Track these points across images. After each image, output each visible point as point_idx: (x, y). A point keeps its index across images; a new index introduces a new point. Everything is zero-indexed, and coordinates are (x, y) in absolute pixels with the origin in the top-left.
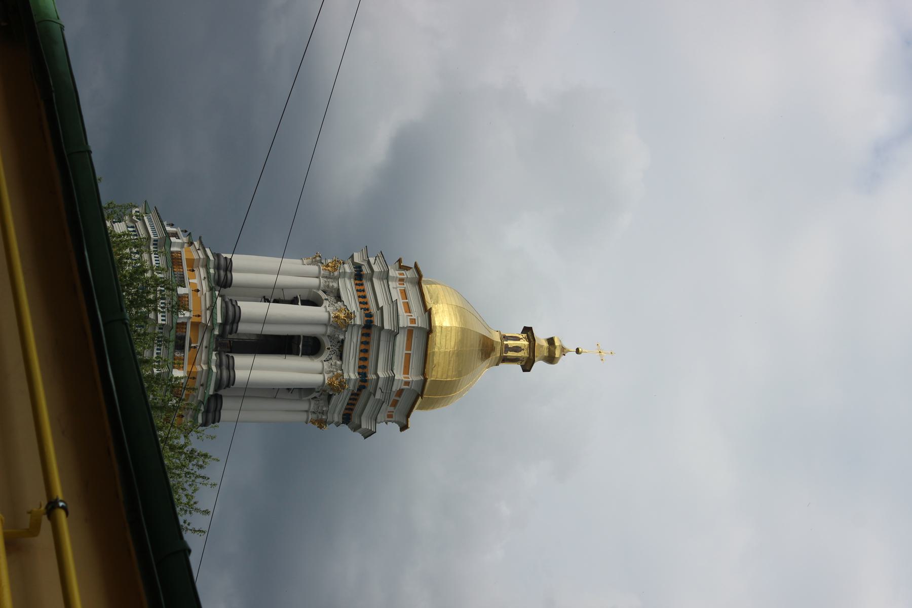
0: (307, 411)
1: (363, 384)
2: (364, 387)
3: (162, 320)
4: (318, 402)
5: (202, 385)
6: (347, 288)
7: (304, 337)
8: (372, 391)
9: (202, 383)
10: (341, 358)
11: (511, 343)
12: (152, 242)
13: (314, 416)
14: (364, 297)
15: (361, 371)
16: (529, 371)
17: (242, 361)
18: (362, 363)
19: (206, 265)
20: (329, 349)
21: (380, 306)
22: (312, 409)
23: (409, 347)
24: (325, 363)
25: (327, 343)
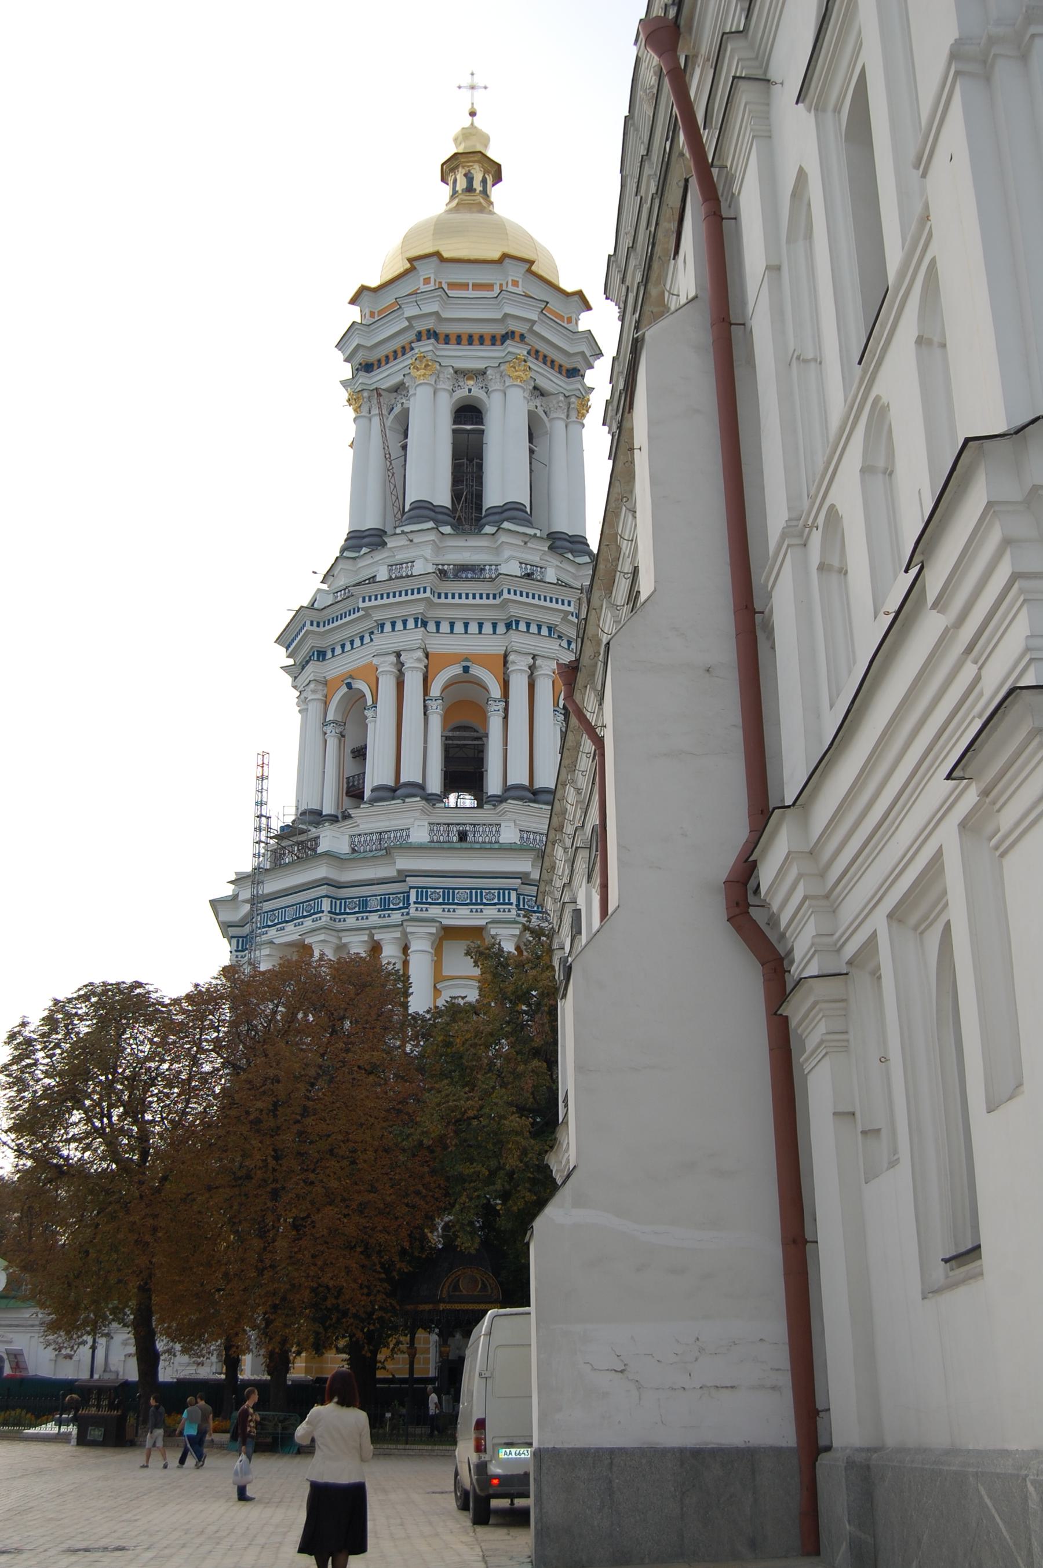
0: (566, 426)
2: (522, 337)
3: (425, 592)
4: (552, 409)
5: (526, 543)
6: (385, 377)
7: (455, 422)
9: (523, 544)
12: (314, 628)
13: (573, 415)
14: (395, 352)
15: (498, 342)
16: (499, 166)
17: (493, 496)
18: (488, 341)
19: (354, 558)
20: (470, 390)
21: (406, 324)
23: (464, 286)
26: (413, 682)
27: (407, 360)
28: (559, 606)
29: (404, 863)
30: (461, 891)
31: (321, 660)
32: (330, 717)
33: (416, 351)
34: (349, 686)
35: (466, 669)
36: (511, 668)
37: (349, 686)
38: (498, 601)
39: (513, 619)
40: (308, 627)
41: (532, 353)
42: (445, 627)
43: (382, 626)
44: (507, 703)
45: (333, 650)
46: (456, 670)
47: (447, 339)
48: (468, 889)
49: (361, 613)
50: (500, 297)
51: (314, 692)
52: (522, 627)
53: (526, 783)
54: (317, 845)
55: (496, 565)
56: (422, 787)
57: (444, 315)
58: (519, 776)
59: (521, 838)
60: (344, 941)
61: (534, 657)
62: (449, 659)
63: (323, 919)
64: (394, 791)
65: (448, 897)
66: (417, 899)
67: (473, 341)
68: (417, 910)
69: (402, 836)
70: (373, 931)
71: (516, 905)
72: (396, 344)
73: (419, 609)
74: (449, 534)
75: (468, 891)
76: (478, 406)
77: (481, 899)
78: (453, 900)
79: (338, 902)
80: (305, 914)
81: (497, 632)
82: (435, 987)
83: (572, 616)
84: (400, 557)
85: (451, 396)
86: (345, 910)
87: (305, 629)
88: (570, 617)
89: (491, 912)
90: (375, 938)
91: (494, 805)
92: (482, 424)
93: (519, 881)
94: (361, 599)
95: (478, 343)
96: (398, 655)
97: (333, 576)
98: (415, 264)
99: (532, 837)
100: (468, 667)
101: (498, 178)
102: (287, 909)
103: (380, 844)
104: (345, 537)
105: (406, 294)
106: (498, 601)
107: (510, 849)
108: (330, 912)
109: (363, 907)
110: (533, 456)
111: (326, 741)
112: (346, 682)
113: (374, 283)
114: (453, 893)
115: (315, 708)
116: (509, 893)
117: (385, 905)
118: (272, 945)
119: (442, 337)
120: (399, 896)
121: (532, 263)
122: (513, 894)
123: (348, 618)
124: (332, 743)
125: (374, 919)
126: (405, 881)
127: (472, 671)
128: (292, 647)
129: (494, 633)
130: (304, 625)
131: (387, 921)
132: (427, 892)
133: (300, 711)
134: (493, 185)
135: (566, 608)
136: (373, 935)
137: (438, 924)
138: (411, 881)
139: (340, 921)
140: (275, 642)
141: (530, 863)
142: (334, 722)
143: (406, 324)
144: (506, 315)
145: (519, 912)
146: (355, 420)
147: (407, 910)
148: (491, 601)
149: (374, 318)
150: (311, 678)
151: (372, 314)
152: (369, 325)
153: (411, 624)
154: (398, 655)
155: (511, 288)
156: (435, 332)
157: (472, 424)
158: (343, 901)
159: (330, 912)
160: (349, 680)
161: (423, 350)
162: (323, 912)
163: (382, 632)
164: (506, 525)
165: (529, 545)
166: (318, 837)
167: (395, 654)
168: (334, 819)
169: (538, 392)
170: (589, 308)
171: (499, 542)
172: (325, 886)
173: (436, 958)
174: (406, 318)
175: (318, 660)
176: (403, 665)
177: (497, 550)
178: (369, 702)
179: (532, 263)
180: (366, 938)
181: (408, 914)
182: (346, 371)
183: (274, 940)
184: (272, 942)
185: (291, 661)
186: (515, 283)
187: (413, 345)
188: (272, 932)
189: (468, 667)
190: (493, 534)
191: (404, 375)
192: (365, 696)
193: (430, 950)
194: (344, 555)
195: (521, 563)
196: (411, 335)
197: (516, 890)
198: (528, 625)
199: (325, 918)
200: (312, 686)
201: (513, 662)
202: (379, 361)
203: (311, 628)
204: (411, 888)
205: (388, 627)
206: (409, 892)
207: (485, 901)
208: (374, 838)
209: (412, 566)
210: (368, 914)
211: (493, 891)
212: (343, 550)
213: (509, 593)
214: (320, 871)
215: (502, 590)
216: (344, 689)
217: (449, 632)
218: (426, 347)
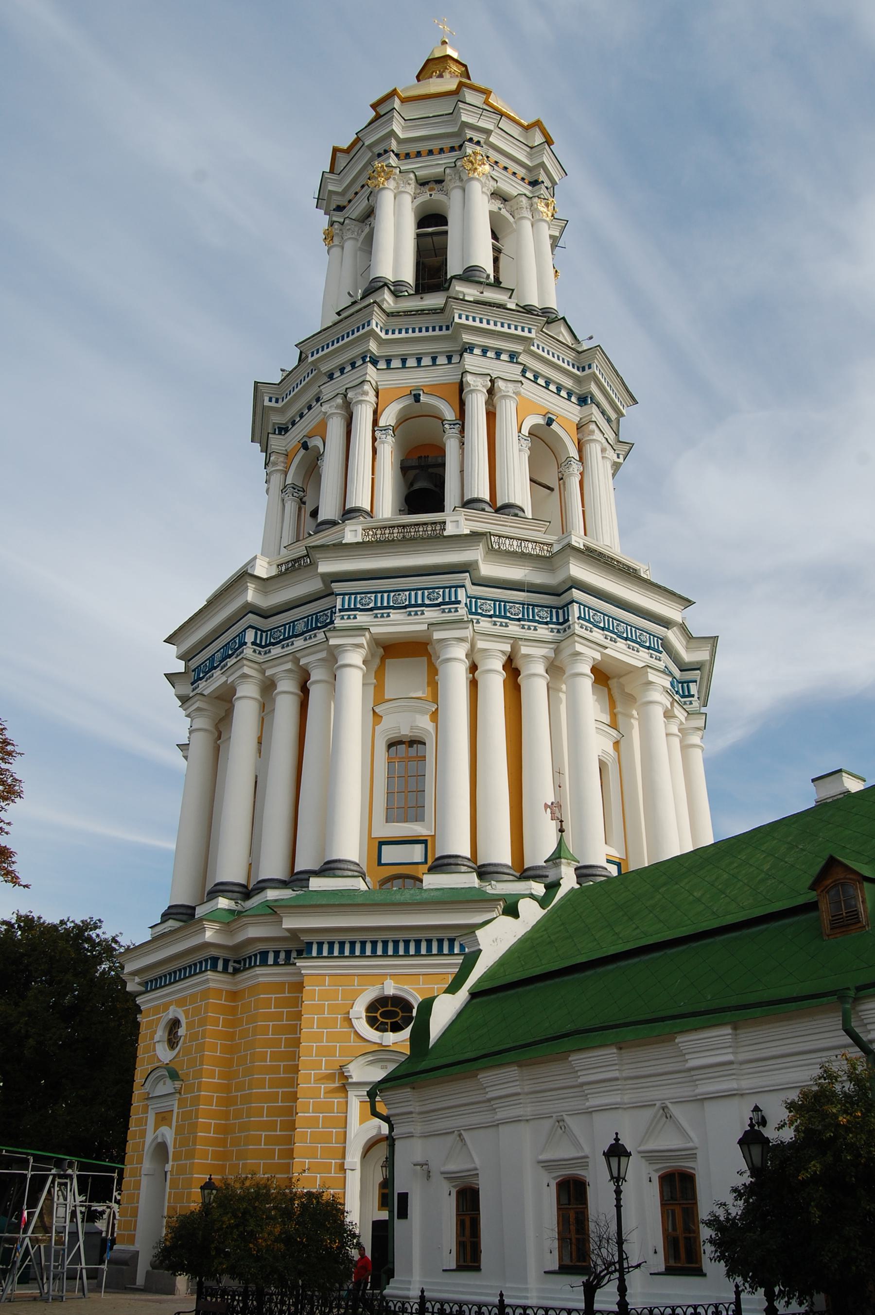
20: (500, 209)
24: (517, 216)
32: (382, 423)
42: (529, 375)
49: (444, 332)
57: (492, 139)
60: (481, 644)
72: (435, 145)
80: (427, 602)
87: (367, 329)
89: (644, 654)
96: (492, 381)
102: (392, 594)
109: (501, 613)
112: (413, 393)
125: (514, 629)
127: (554, 426)
131: (531, 634)
138: (576, 594)
144: (542, 165)
148: (575, 371)
162: (459, 602)
166: (445, 523)
167: (489, 378)
188: (362, 619)
205: (477, 351)
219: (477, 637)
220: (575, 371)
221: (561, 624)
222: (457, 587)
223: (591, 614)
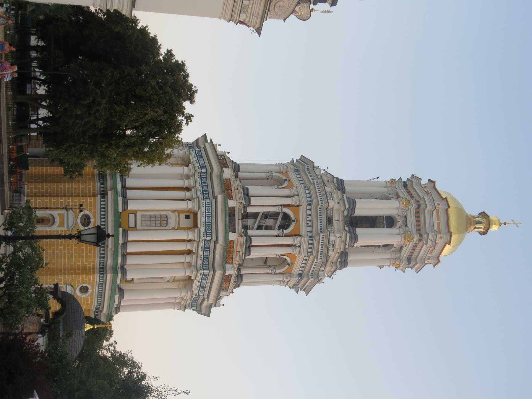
0: (389, 259)
1: (420, 238)
6: (402, 192)
7: (386, 216)
8: (425, 242)
9: (342, 241)
10: (406, 226)
11: (477, 219)
12: (306, 168)
14: (411, 194)
17: (359, 231)
18: (418, 228)
19: (333, 182)
20: (399, 221)
22: (392, 257)
23: (438, 219)
25: (399, 219)
26: (288, 201)
27: (408, 197)
28: (319, 255)
29: (220, 198)
30: (211, 219)
31: (296, 171)
33: (412, 200)
34: (286, 180)
35: (294, 221)
36: (295, 237)
37: (286, 180)
38: (319, 232)
39: (313, 239)
40: (307, 165)
41: (416, 245)
42: (309, 212)
43: (308, 190)
44: (282, 236)
45: (299, 174)
46: (293, 217)
47: (417, 212)
48: (211, 221)
49: (312, 182)
50: (434, 231)
51: (283, 168)
52: (310, 242)
53: (253, 244)
54: (226, 168)
55: (333, 232)
56: (249, 205)
58: (255, 242)
59: (231, 241)
60: (191, 178)
61: (299, 246)
62: (297, 214)
63: (199, 170)
64: (247, 196)
65: (208, 214)
66: (207, 203)
67: (418, 222)
68: (203, 203)
69: (230, 197)
70: (195, 188)
71: (205, 240)
73: (315, 203)
74: (344, 214)
75: (210, 222)
76: (394, 225)
77: (207, 226)
78: (207, 216)
79: (205, 175)
80: (200, 164)
81: (308, 233)
82: (176, 211)
83: (316, 261)
84: (335, 196)
85: (396, 214)
86: (203, 177)
88: (316, 260)
89: (203, 229)
90: (192, 189)
91: (243, 232)
92: (387, 227)
93: (215, 240)
94: (317, 181)
95: (417, 224)
97: (327, 175)
98: (445, 200)
99: (232, 245)
100: (294, 221)
101: (482, 234)
103: (227, 189)
104: (342, 179)
105: (434, 198)
106: (319, 232)
107: (226, 236)
108: (201, 172)
109: (203, 184)
110: (377, 248)
111: (265, 173)
113: (436, 186)
114: (210, 216)
115: (277, 169)
116: (210, 236)
117: (204, 192)
118: (189, 154)
119: (417, 210)
120: (208, 197)
121: (450, 244)
122: (210, 238)
123: (310, 178)
124: (264, 175)
125: (199, 188)
126: (213, 198)
128: (300, 161)
129: (308, 232)
130: (307, 164)
132: (210, 206)
133: (276, 164)
134: (479, 232)
135: (319, 257)
136: (193, 188)
137: (198, 210)
139: (198, 176)
140: (301, 155)
141: (221, 244)
142: (272, 175)
143: (422, 197)
144: (428, 234)
145: (204, 240)
146: (385, 181)
147: (203, 199)
149: (424, 187)
150: (288, 167)
151: (425, 187)
152: (421, 185)
153: (309, 199)
154: (298, 195)
155: (438, 236)
156: (420, 207)
157: (386, 223)
158: (205, 177)
159: (201, 172)
160: (288, 180)
161: (413, 202)
162: (201, 169)
163: (305, 190)
164: (348, 235)
165: (342, 243)
166: (229, 168)
168: (236, 177)
169: (402, 248)
170: (434, 266)
171: (342, 232)
172: (210, 170)
173: (186, 211)
174: (424, 197)
175: (295, 170)
176: (294, 197)
177: (339, 231)
178: (280, 187)
179: (450, 244)
180: (192, 185)
181: (201, 200)
182: (404, 180)
183: (191, 155)
184: (190, 154)
185: (295, 162)
186: (441, 238)
187: (414, 199)
188: (194, 154)
189: (294, 221)
190: (345, 230)
191: (403, 197)
192: (282, 185)
193: (188, 208)
194: (335, 178)
195: (334, 241)
196: (418, 199)
197: (212, 239)
198: (311, 244)
199: (199, 170)
200: (285, 167)
201: (297, 238)
202: (408, 189)
203: (306, 167)
204: (211, 200)
206: (209, 200)
207: (207, 227)
208: (229, 187)
209: (331, 200)
210: (201, 185)
211: (211, 230)
212: (337, 178)
213: (323, 236)
214: (216, 169)
215: (323, 233)
216: (284, 178)
217: (308, 214)
218: (414, 206)
219: (193, 176)
220: (319, 230)
221: (204, 199)
222: (206, 169)
223: (209, 207)
